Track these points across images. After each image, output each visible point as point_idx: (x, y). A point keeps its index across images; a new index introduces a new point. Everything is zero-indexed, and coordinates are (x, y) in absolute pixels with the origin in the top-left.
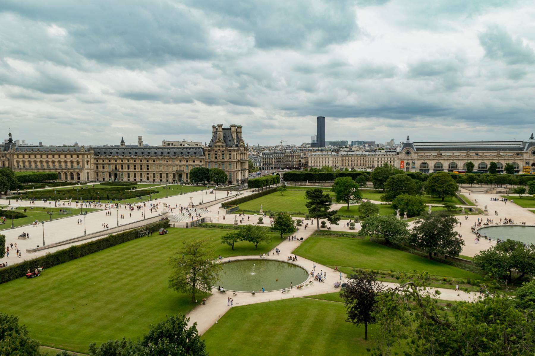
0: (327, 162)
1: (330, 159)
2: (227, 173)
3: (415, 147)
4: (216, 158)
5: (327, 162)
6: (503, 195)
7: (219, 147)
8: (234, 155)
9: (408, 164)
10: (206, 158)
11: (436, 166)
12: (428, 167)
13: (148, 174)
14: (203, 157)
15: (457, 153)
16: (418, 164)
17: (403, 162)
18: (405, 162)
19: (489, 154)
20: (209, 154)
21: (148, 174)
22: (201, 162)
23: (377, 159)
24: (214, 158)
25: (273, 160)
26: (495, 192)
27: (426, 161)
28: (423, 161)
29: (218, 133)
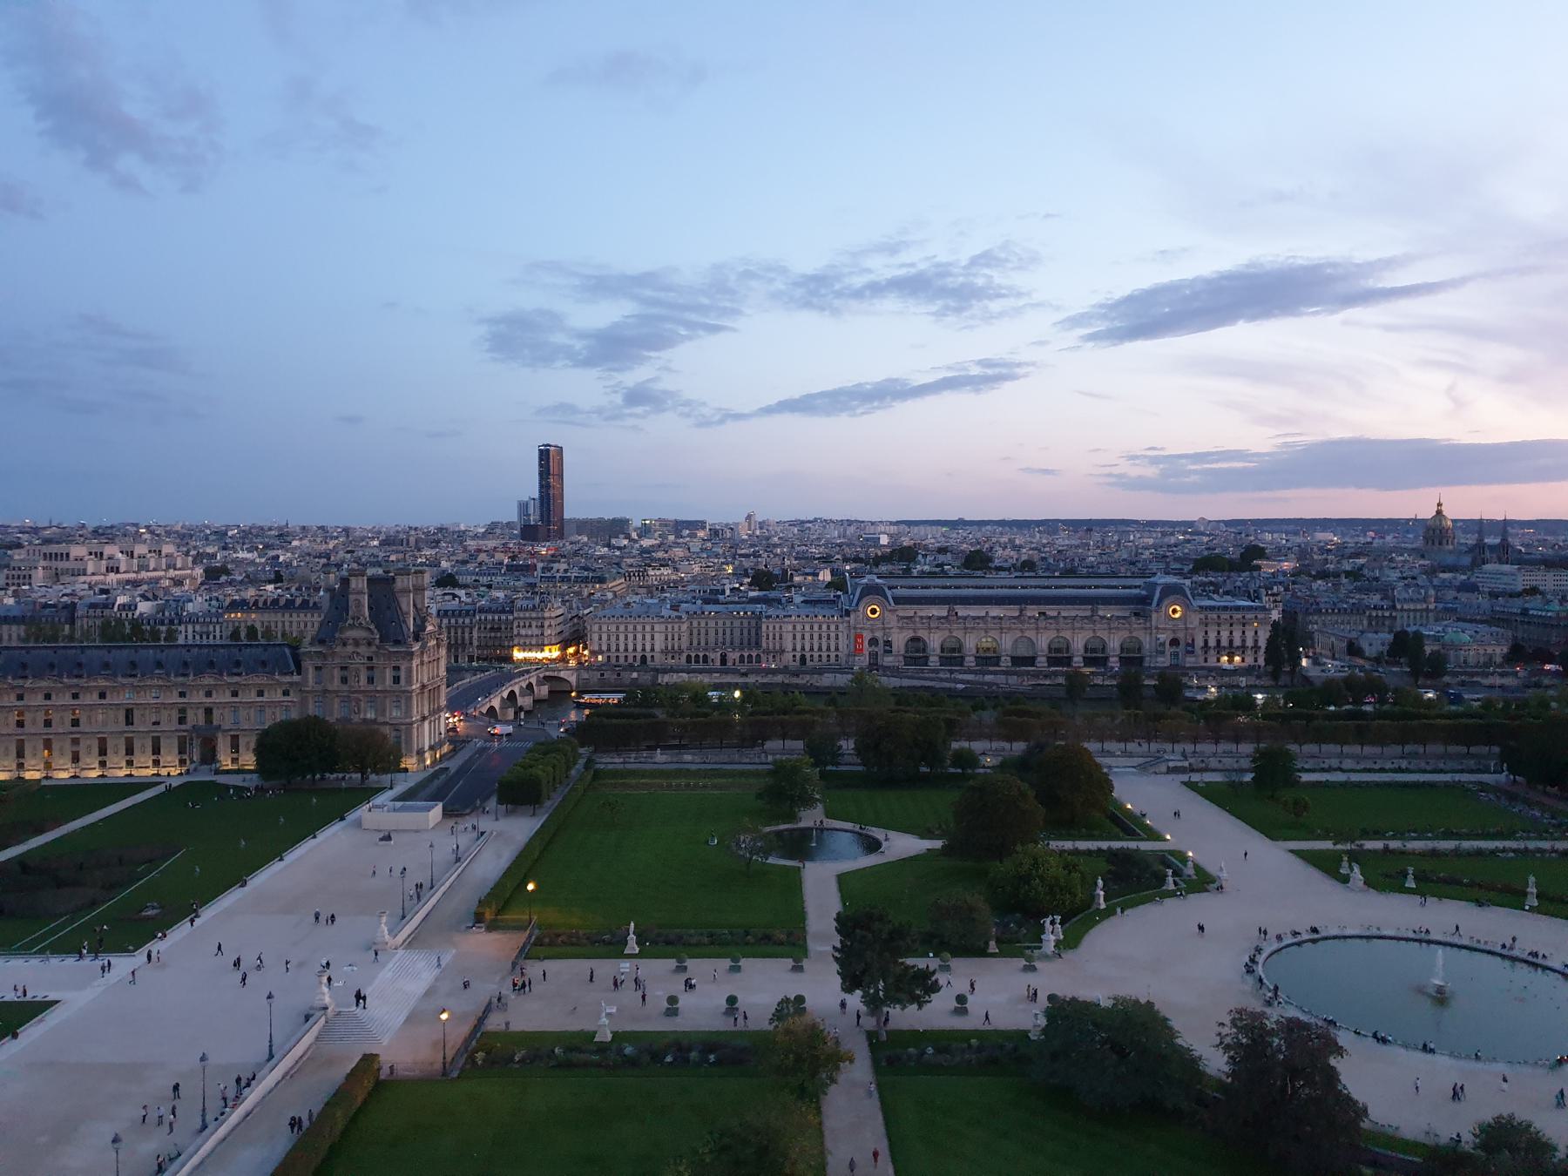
0: (648, 637)
1: (657, 628)
2: (387, 730)
3: (889, 593)
4: (344, 680)
5: (648, 637)
6: (1185, 778)
7: (357, 643)
8: (409, 670)
9: (873, 642)
10: (306, 680)
11: (947, 645)
12: (924, 650)
13: (75, 742)
14: (296, 678)
15: (996, 611)
16: (899, 640)
17: (861, 636)
18: (867, 636)
19: (1073, 614)
20: (318, 668)
21: (75, 742)
22: (286, 693)
23: (790, 627)
24: (337, 681)
25: (475, 634)
26: (1163, 768)
27: (921, 634)
28: (911, 634)
29: (352, 597)
